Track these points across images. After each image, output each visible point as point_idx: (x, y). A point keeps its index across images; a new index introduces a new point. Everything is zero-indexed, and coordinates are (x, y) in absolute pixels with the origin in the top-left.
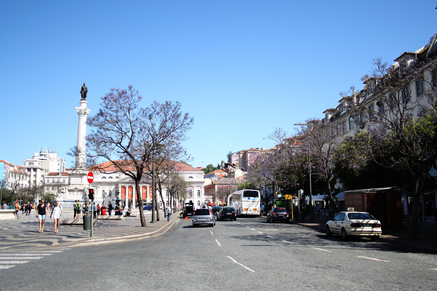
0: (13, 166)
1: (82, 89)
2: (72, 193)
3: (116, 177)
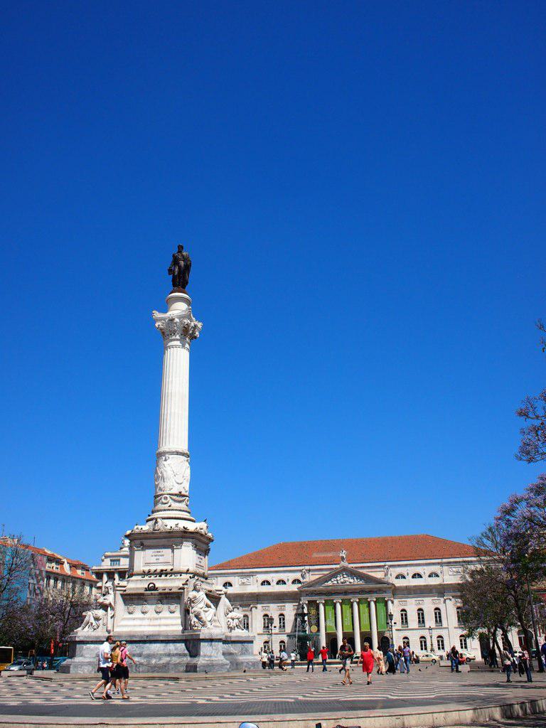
0: (59, 562)
1: (176, 261)
2: (138, 609)
3: (294, 582)
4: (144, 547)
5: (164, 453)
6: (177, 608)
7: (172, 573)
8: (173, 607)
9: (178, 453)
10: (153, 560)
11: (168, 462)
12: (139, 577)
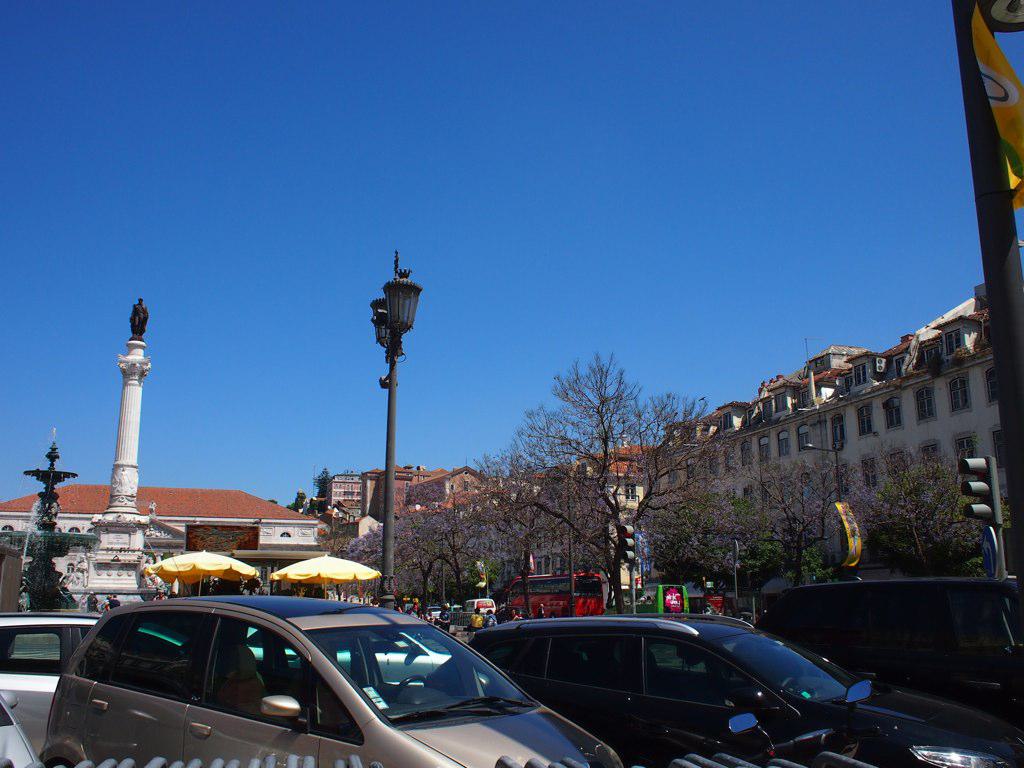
1: (136, 311)
4: (108, 532)
5: (122, 466)
6: (133, 573)
7: (129, 550)
8: (130, 573)
9: (133, 466)
10: (115, 541)
11: (126, 472)
12: (104, 552)
